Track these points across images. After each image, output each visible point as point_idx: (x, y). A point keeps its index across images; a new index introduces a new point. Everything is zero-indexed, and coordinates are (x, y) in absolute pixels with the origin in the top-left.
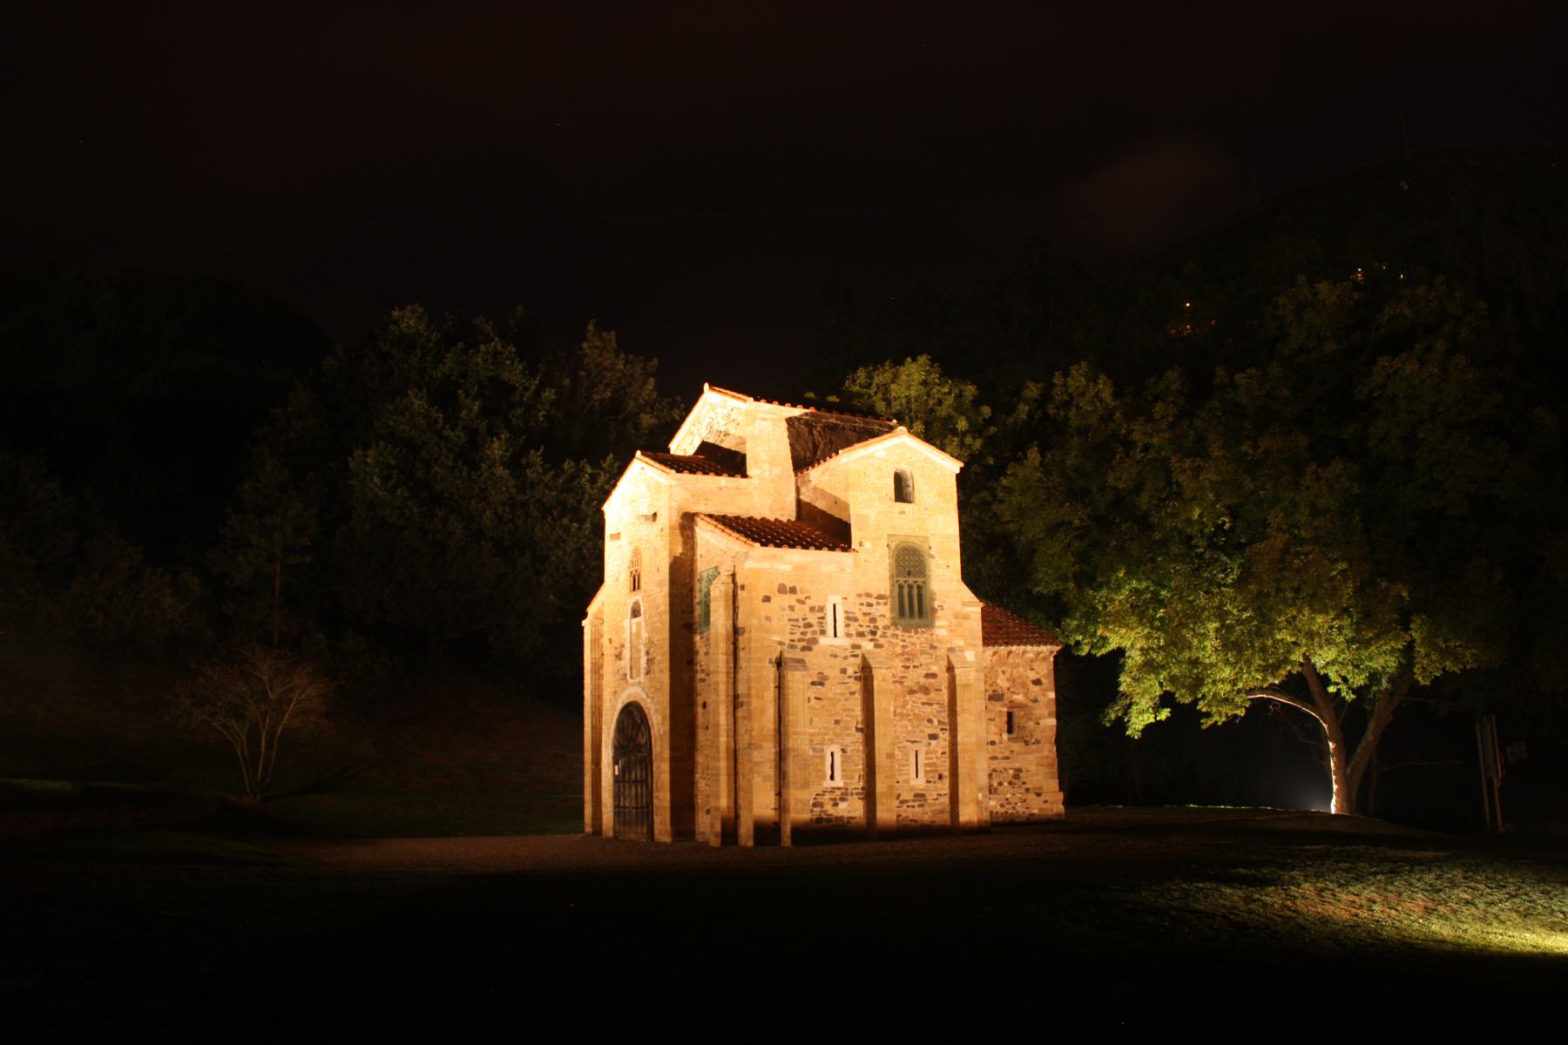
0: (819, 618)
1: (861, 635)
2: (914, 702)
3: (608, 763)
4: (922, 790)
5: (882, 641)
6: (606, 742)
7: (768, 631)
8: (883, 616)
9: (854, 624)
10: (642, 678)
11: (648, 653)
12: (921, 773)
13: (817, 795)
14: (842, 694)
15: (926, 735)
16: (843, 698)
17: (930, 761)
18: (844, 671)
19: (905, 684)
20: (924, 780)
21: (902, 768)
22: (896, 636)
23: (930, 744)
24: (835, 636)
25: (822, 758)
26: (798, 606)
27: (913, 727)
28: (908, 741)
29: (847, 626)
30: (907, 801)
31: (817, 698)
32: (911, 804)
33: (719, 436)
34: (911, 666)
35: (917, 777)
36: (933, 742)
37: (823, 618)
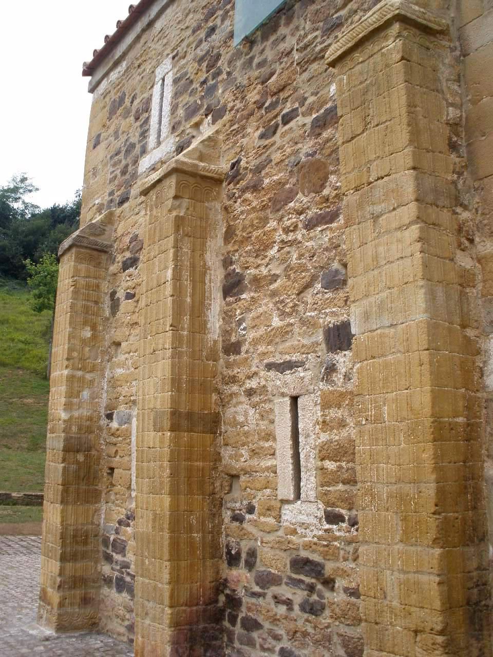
0: (141, 126)
2: (287, 231)
4: (308, 546)
12: (309, 482)
13: (120, 522)
15: (320, 337)
17: (336, 436)
19: (267, 181)
20: (319, 509)
21: (254, 462)
23: (331, 369)
25: (127, 435)
27: (283, 314)
28: (269, 367)
30: (275, 580)
31: (130, 296)
32: (285, 591)
34: (279, 118)
35: (298, 496)
36: (343, 360)
37: (147, 120)
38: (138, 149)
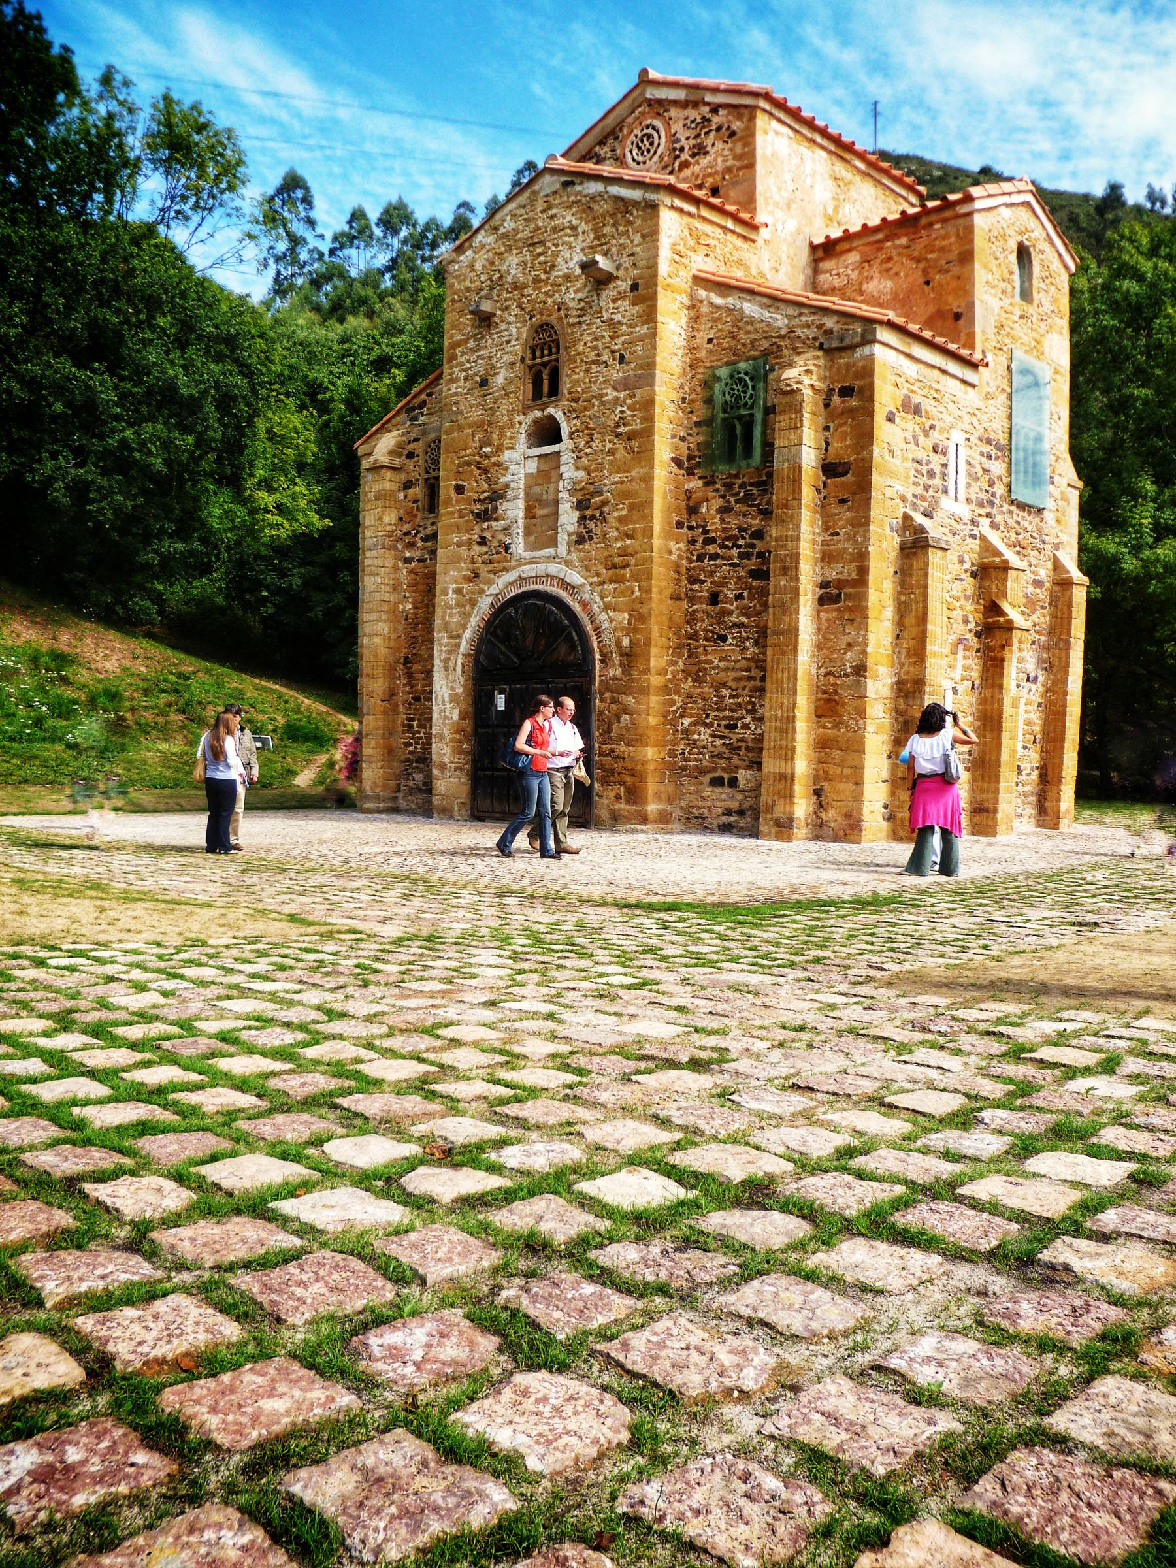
1: (981, 504)
3: (454, 698)
5: (999, 519)
6: (446, 661)
7: (892, 474)
8: (1000, 478)
9: (975, 486)
10: (562, 549)
11: (580, 505)
14: (957, 599)
16: (958, 604)
18: (961, 561)
22: (1010, 512)
24: (956, 499)
26: (921, 439)
29: (968, 485)
33: (678, 157)
37: (945, 466)
38: (937, 481)
